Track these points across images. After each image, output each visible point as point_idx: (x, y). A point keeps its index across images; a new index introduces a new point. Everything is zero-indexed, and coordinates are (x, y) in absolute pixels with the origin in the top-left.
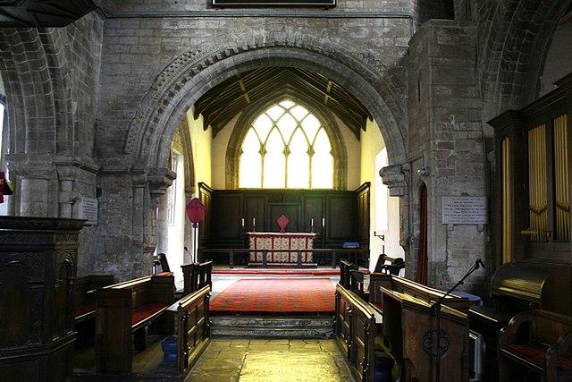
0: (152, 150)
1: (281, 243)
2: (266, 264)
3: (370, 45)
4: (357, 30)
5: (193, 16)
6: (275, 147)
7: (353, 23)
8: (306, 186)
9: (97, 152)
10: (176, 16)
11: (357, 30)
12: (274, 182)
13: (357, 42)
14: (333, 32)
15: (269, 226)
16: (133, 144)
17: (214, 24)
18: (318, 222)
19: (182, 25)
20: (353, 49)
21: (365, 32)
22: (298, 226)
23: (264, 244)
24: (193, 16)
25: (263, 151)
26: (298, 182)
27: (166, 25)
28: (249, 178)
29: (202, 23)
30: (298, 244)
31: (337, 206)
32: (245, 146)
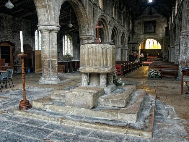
1: (152, 57)
4: (158, 36)
5: (141, 35)
8: (156, 49)
9: (132, 49)
12: (151, 48)
15: (150, 55)
17: (143, 36)
19: (140, 36)
22: (155, 55)
23: (149, 57)
24: (141, 35)
25: (149, 43)
26: (155, 48)
27: (138, 36)
28: (147, 47)
29: (142, 35)
32: (146, 42)
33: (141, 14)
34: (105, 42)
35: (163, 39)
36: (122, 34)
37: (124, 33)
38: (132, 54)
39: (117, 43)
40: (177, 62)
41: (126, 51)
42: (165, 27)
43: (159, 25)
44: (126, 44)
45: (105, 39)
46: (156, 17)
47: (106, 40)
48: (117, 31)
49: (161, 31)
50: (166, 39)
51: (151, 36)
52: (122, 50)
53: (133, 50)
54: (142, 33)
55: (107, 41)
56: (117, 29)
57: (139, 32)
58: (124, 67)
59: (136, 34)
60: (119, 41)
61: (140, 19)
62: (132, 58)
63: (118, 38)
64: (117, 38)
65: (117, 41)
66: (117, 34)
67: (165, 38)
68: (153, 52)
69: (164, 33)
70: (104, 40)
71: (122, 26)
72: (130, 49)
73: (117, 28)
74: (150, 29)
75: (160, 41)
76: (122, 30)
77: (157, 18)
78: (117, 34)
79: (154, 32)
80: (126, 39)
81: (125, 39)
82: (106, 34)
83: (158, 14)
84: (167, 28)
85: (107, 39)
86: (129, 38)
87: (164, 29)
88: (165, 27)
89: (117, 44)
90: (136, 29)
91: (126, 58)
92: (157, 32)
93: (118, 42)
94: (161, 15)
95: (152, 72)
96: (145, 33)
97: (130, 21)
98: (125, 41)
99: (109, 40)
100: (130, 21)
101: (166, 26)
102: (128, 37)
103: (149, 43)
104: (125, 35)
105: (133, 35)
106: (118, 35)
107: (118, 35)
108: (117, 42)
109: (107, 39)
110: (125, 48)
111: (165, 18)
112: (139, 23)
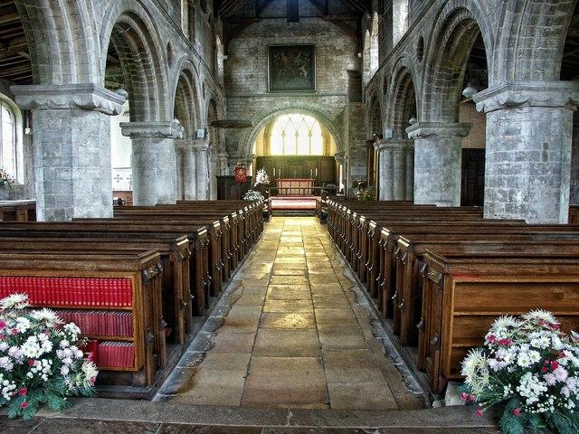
0: (247, 148)
2: (287, 196)
3: (330, 107)
4: (324, 101)
5: (261, 96)
6: (290, 133)
7: (323, 98)
8: (307, 154)
10: (254, 97)
11: (324, 101)
12: (290, 152)
13: (324, 106)
14: (315, 102)
15: (287, 176)
16: (240, 148)
18: (314, 173)
20: (323, 109)
21: (327, 102)
22: (305, 176)
23: (286, 185)
24: (261, 96)
25: (284, 134)
27: (251, 100)
29: (264, 99)
30: (304, 185)
31: (325, 164)
33: (258, 18)
34: (57, 82)
35: (342, 113)
36: (181, 80)
37: (187, 71)
38: (226, 172)
39: (153, 113)
40: (509, 209)
41: (203, 154)
42: (348, 71)
43: (328, 63)
44: (199, 127)
45: (58, 70)
46: (313, 32)
47: (67, 74)
48: (151, 44)
49: (335, 80)
50: (355, 114)
51: (300, 103)
52: (182, 153)
53: (229, 158)
54: (262, 89)
55: (75, 81)
56: (154, 36)
57: (251, 88)
58: (181, 272)
59: (240, 94)
60: (162, 105)
61: (255, 35)
62: (230, 188)
63: (161, 85)
64: (151, 84)
65: (152, 99)
66: (151, 62)
67: (354, 110)
68: (296, 168)
69: (346, 91)
70: (51, 71)
71: (180, 32)
72: (219, 151)
73: (150, 27)
74: (293, 68)
75: (333, 124)
76: (180, 56)
77: (319, 37)
78: (151, 62)
79: (311, 88)
80: (203, 104)
81: (197, 102)
82: (60, 28)
83: (322, 22)
84: (356, 75)
85: (75, 69)
86: (213, 103)
87: (345, 77)
88: (348, 71)
89: (153, 118)
90: (241, 74)
91: (203, 187)
92: (321, 88)
93: (158, 108)
94: (333, 26)
95: (539, 370)
96: (274, 89)
97: (219, 42)
98: (198, 111)
99: (84, 71)
100: (219, 42)
101: (351, 66)
102: (208, 97)
103: (284, 134)
104: (197, 85)
105: (227, 96)
106: (158, 71)
107: (158, 71)
108: (153, 105)
109: (75, 69)
110: (198, 146)
111: (348, 40)
112: (253, 52)
